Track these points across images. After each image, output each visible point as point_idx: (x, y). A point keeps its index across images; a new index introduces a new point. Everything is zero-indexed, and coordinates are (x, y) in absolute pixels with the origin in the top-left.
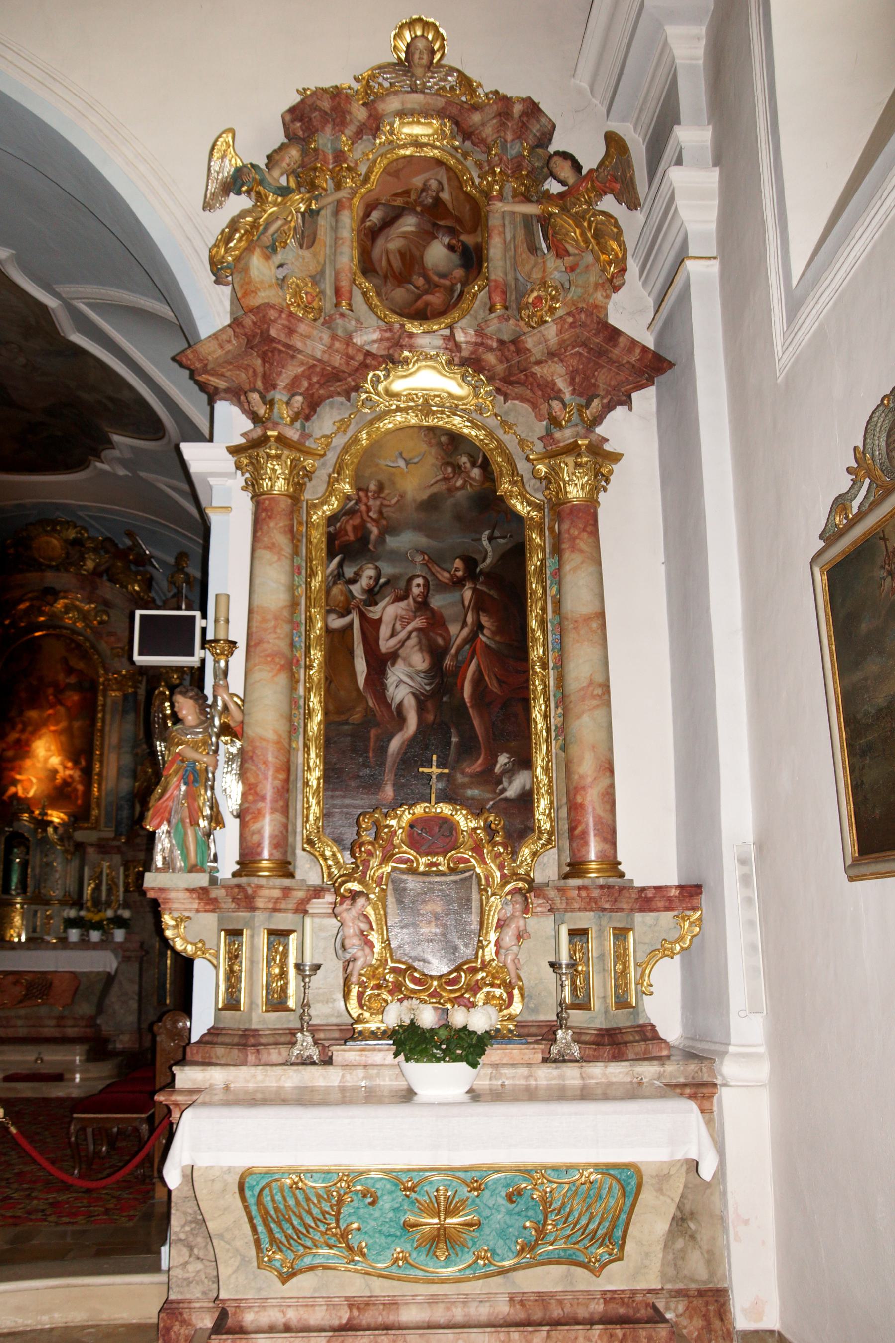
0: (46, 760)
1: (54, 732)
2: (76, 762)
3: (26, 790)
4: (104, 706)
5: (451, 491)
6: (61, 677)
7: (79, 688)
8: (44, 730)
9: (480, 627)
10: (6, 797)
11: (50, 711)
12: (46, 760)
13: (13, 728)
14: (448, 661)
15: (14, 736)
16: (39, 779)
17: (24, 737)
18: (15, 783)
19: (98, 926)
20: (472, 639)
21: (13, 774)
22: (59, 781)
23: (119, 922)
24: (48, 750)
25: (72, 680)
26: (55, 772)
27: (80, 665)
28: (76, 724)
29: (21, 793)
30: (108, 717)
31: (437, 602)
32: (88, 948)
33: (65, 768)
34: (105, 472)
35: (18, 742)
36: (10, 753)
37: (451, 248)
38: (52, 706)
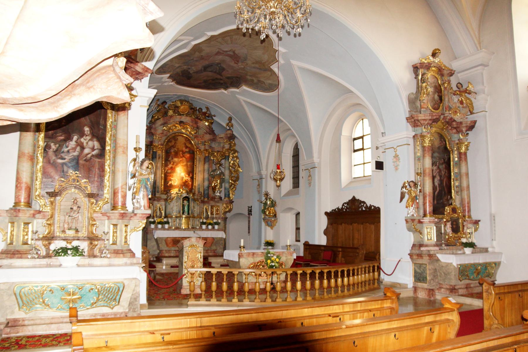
0: (180, 174)
1: (182, 165)
2: (189, 175)
3: (174, 183)
4: (196, 159)
5: (441, 146)
6: (184, 149)
7: (189, 152)
8: (179, 165)
9: (445, 172)
10: (168, 185)
11: (181, 159)
12: (180, 174)
13: (170, 163)
14: (442, 178)
15: (170, 166)
16: (178, 180)
17: (173, 166)
18: (171, 180)
19: (210, 224)
20: (445, 174)
21: (170, 177)
22: (184, 181)
23: (217, 223)
24: (181, 171)
25: (187, 150)
26: (183, 178)
27: (189, 146)
28: (189, 164)
29: (173, 184)
30: (198, 162)
31: (440, 167)
32: (164, 230)
33: (186, 176)
34: (224, 93)
35: (172, 168)
36: (169, 171)
37: (438, 96)
38: (181, 157)
